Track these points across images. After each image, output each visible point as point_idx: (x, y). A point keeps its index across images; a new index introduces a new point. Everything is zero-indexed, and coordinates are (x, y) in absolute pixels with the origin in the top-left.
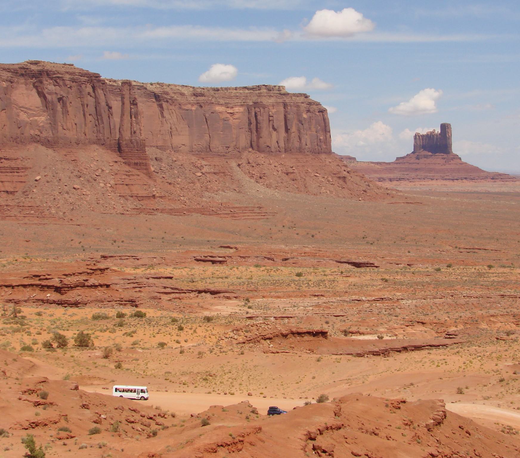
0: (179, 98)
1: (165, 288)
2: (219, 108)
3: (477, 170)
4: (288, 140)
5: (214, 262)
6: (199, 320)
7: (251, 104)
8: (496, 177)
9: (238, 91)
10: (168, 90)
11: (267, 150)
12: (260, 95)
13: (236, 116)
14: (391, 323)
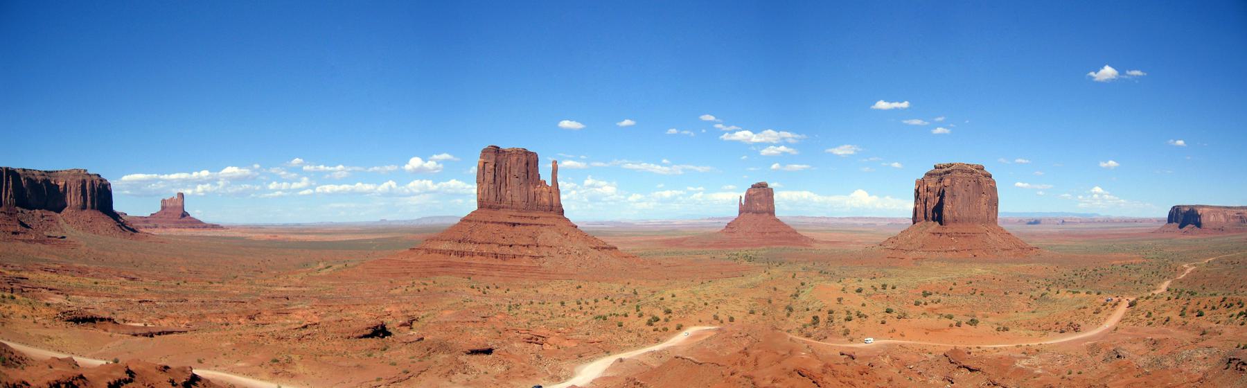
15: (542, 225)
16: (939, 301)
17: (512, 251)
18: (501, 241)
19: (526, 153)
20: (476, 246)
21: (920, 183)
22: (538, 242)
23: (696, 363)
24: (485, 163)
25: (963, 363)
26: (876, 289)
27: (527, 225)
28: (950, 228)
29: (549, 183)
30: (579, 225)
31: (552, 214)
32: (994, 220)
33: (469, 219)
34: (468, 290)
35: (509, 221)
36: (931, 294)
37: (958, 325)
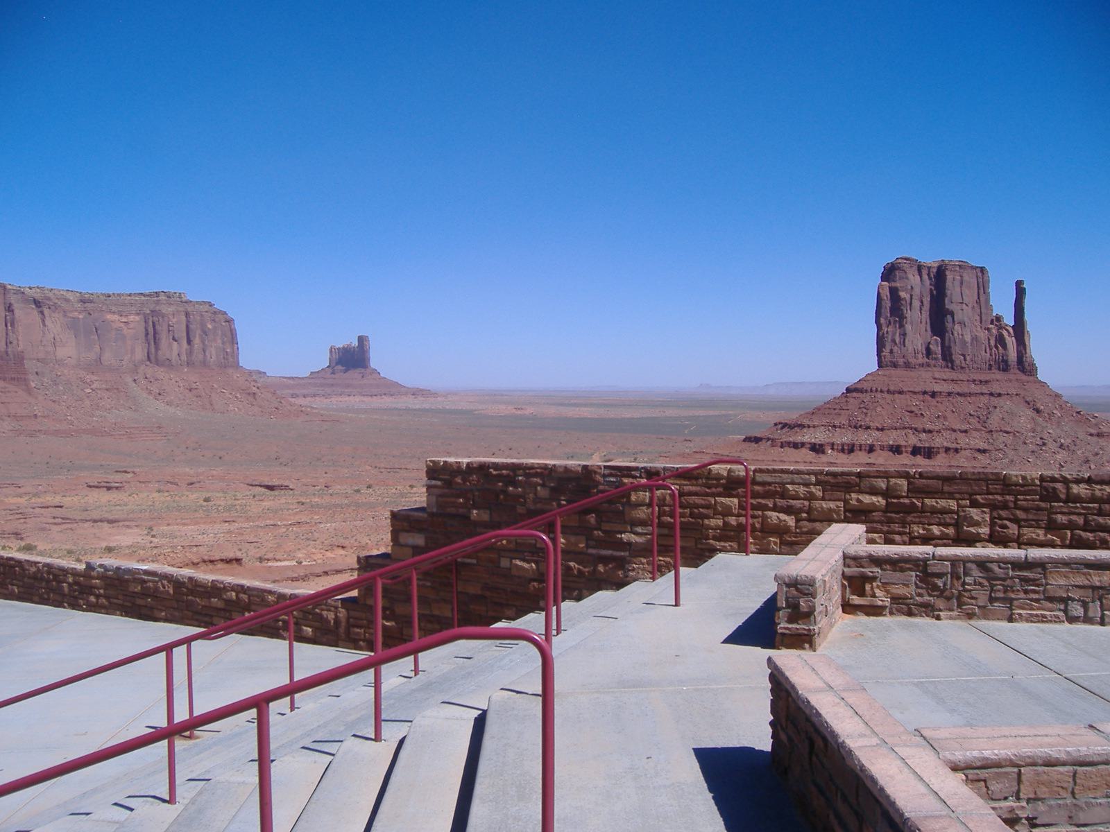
0: (64, 305)
1: (54, 518)
2: (109, 317)
3: (397, 385)
4: (190, 353)
5: (109, 489)
6: (99, 550)
7: (148, 312)
8: (416, 392)
9: (132, 298)
10: (50, 295)
11: (168, 364)
12: (158, 303)
13: (131, 325)
14: (309, 548)
15: (991, 394)
17: (939, 441)
18: (918, 424)
19: (963, 266)
20: (875, 434)
22: (989, 421)
24: (891, 288)
27: (971, 394)
29: (1009, 320)
30: (1066, 395)
31: (1015, 374)
33: (866, 386)
35: (937, 388)
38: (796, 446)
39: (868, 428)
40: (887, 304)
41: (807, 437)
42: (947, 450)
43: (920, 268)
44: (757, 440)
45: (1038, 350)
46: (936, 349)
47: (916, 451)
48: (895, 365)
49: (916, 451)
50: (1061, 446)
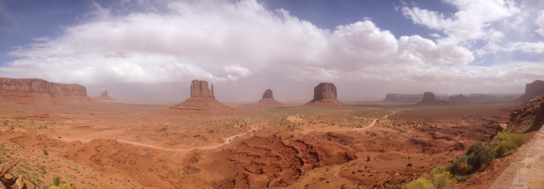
16: (323, 119)
17: (201, 108)
20: (191, 107)
21: (315, 88)
23: (260, 138)
25: (333, 135)
26: (305, 117)
28: (324, 100)
29: (211, 90)
32: (336, 98)
34: (189, 119)
35: (200, 100)
36: (320, 117)
37: (329, 125)
38: (178, 109)
39: (190, 106)
40: (192, 87)
41: (180, 107)
42: (202, 109)
43: (197, 81)
44: (172, 108)
45: (215, 94)
46: (200, 94)
47: (197, 110)
48: (194, 96)
49: (197, 110)
50: (219, 109)
